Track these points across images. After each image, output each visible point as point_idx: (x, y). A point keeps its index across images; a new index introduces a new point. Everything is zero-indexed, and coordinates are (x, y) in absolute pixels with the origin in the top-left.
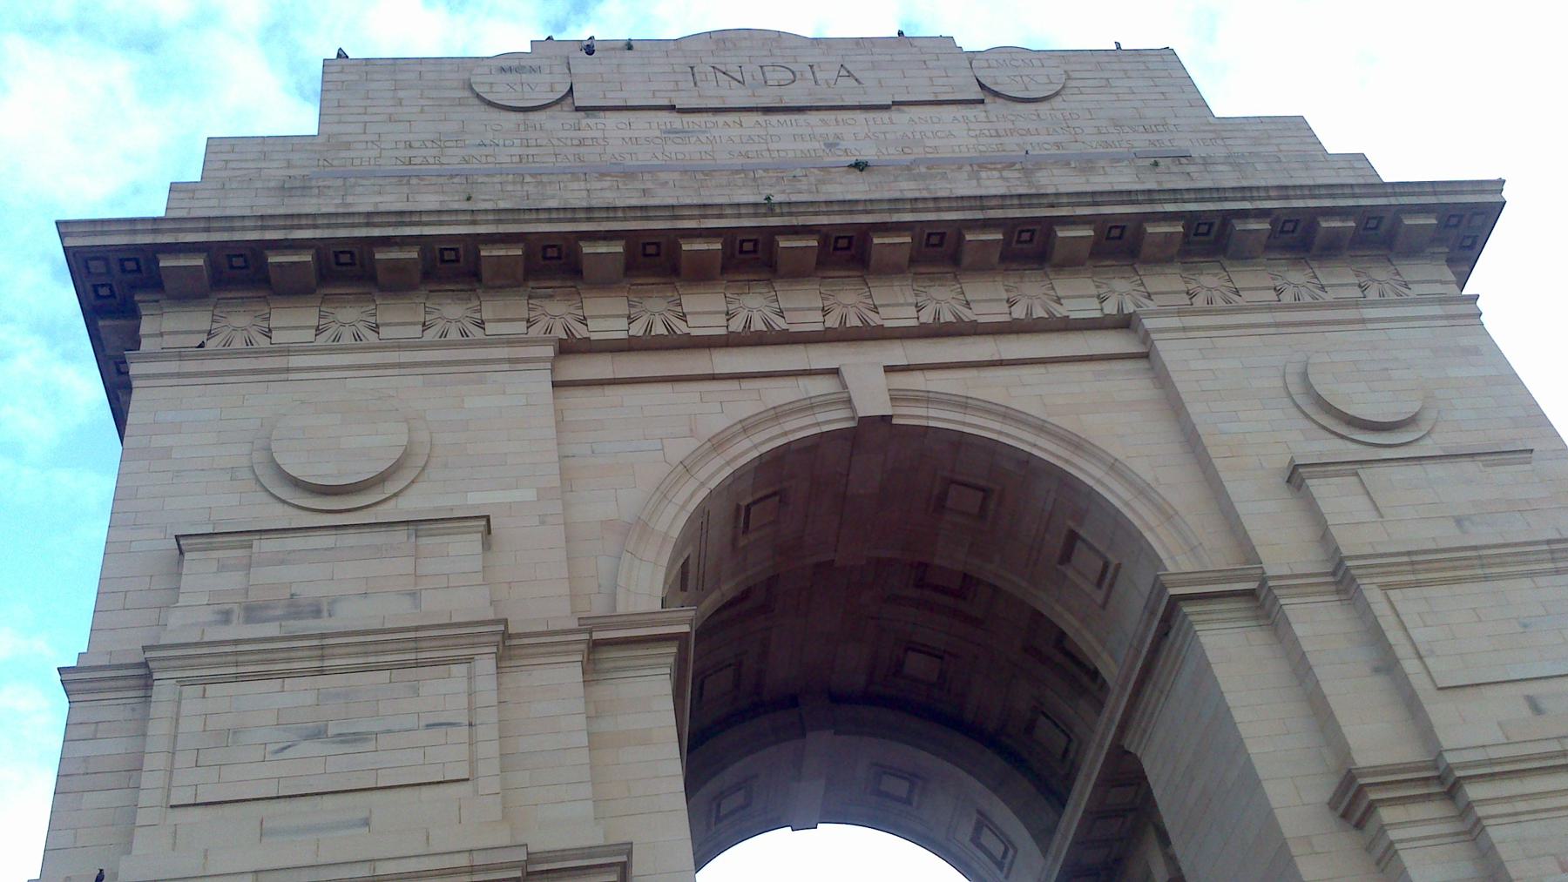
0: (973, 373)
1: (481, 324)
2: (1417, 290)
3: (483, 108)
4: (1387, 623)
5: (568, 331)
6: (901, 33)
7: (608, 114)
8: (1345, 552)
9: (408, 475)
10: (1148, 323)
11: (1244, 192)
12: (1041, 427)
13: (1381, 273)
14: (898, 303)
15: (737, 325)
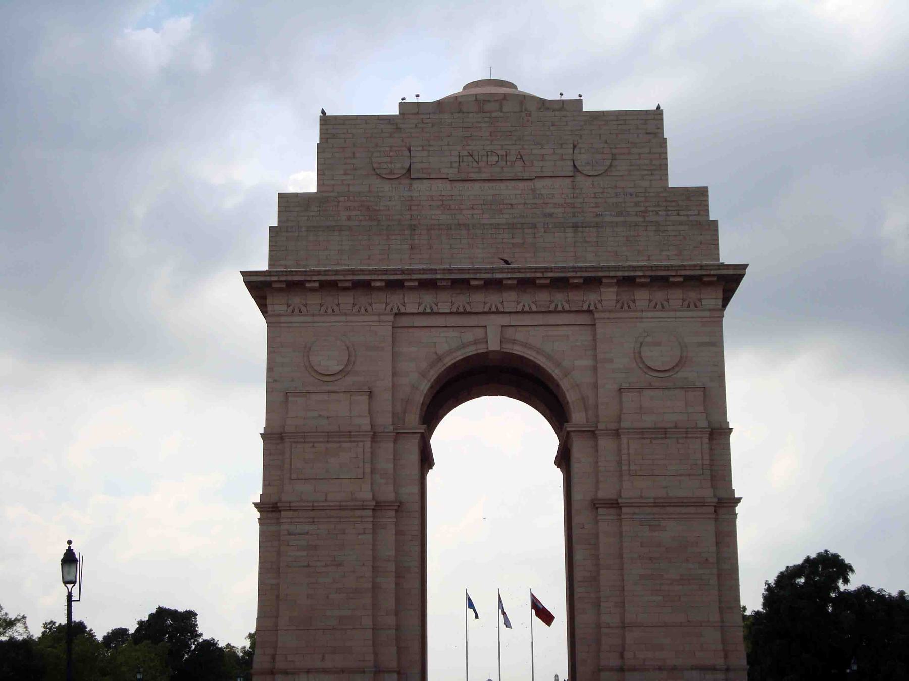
0: (530, 328)
1: (371, 304)
2: (704, 302)
3: (375, 177)
4: (624, 452)
5: (399, 309)
6: (561, 94)
7: (424, 181)
8: (623, 425)
9: (350, 368)
10: (597, 315)
11: (641, 268)
12: (549, 357)
13: (693, 295)
14: (510, 300)
15: (454, 310)
